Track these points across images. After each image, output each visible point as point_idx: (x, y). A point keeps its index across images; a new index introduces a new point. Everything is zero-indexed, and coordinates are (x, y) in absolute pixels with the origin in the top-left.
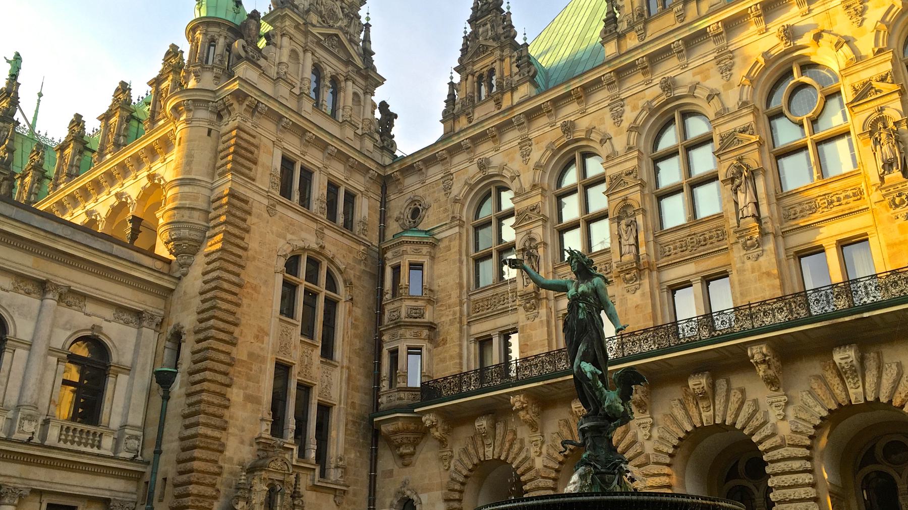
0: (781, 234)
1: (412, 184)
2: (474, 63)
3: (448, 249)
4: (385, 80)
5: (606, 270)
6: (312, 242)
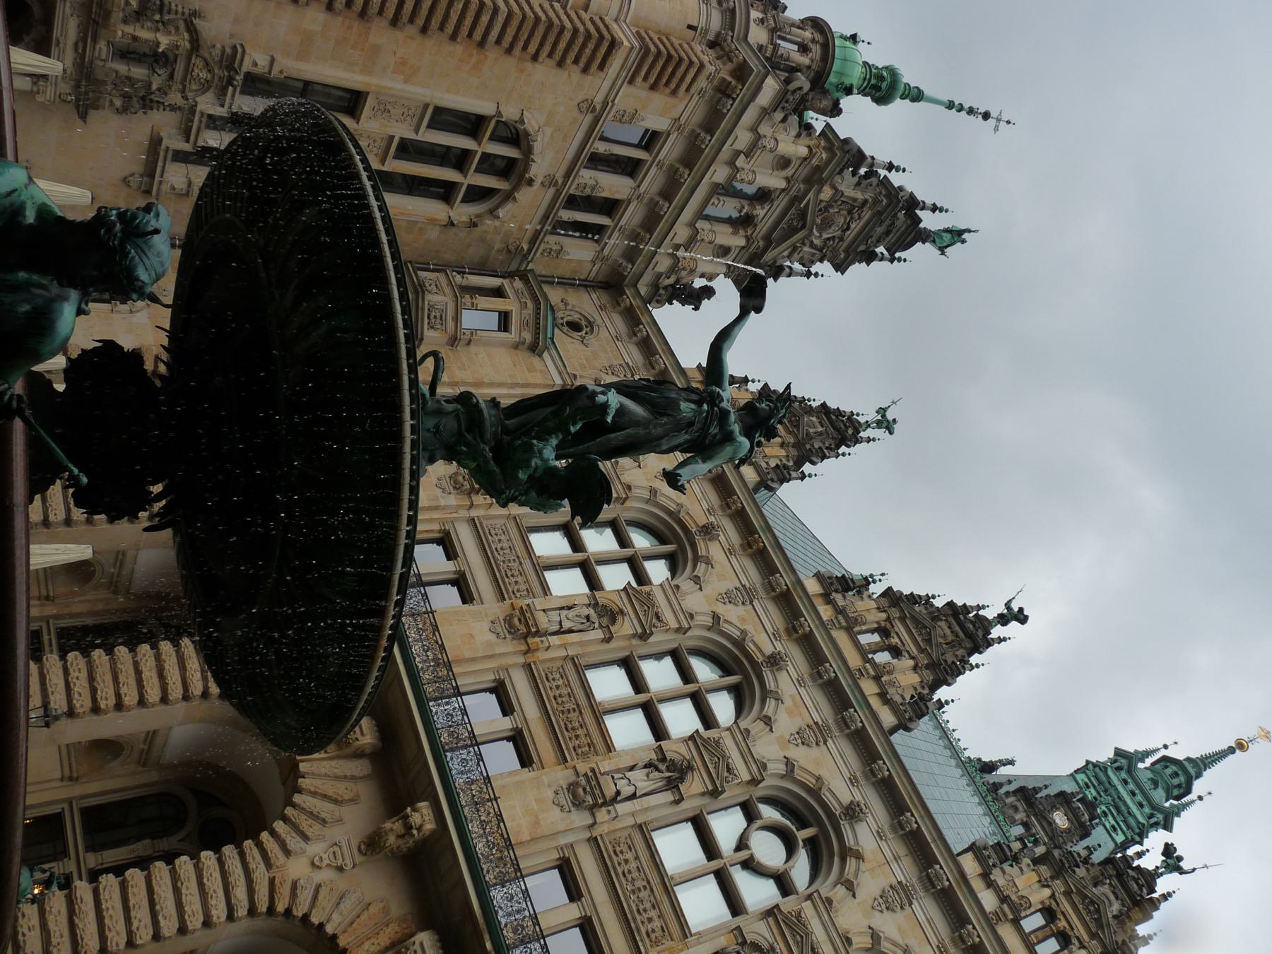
0: (594, 835)
1: (616, 323)
3: (531, 369)
5: (518, 591)
6: (538, 169)
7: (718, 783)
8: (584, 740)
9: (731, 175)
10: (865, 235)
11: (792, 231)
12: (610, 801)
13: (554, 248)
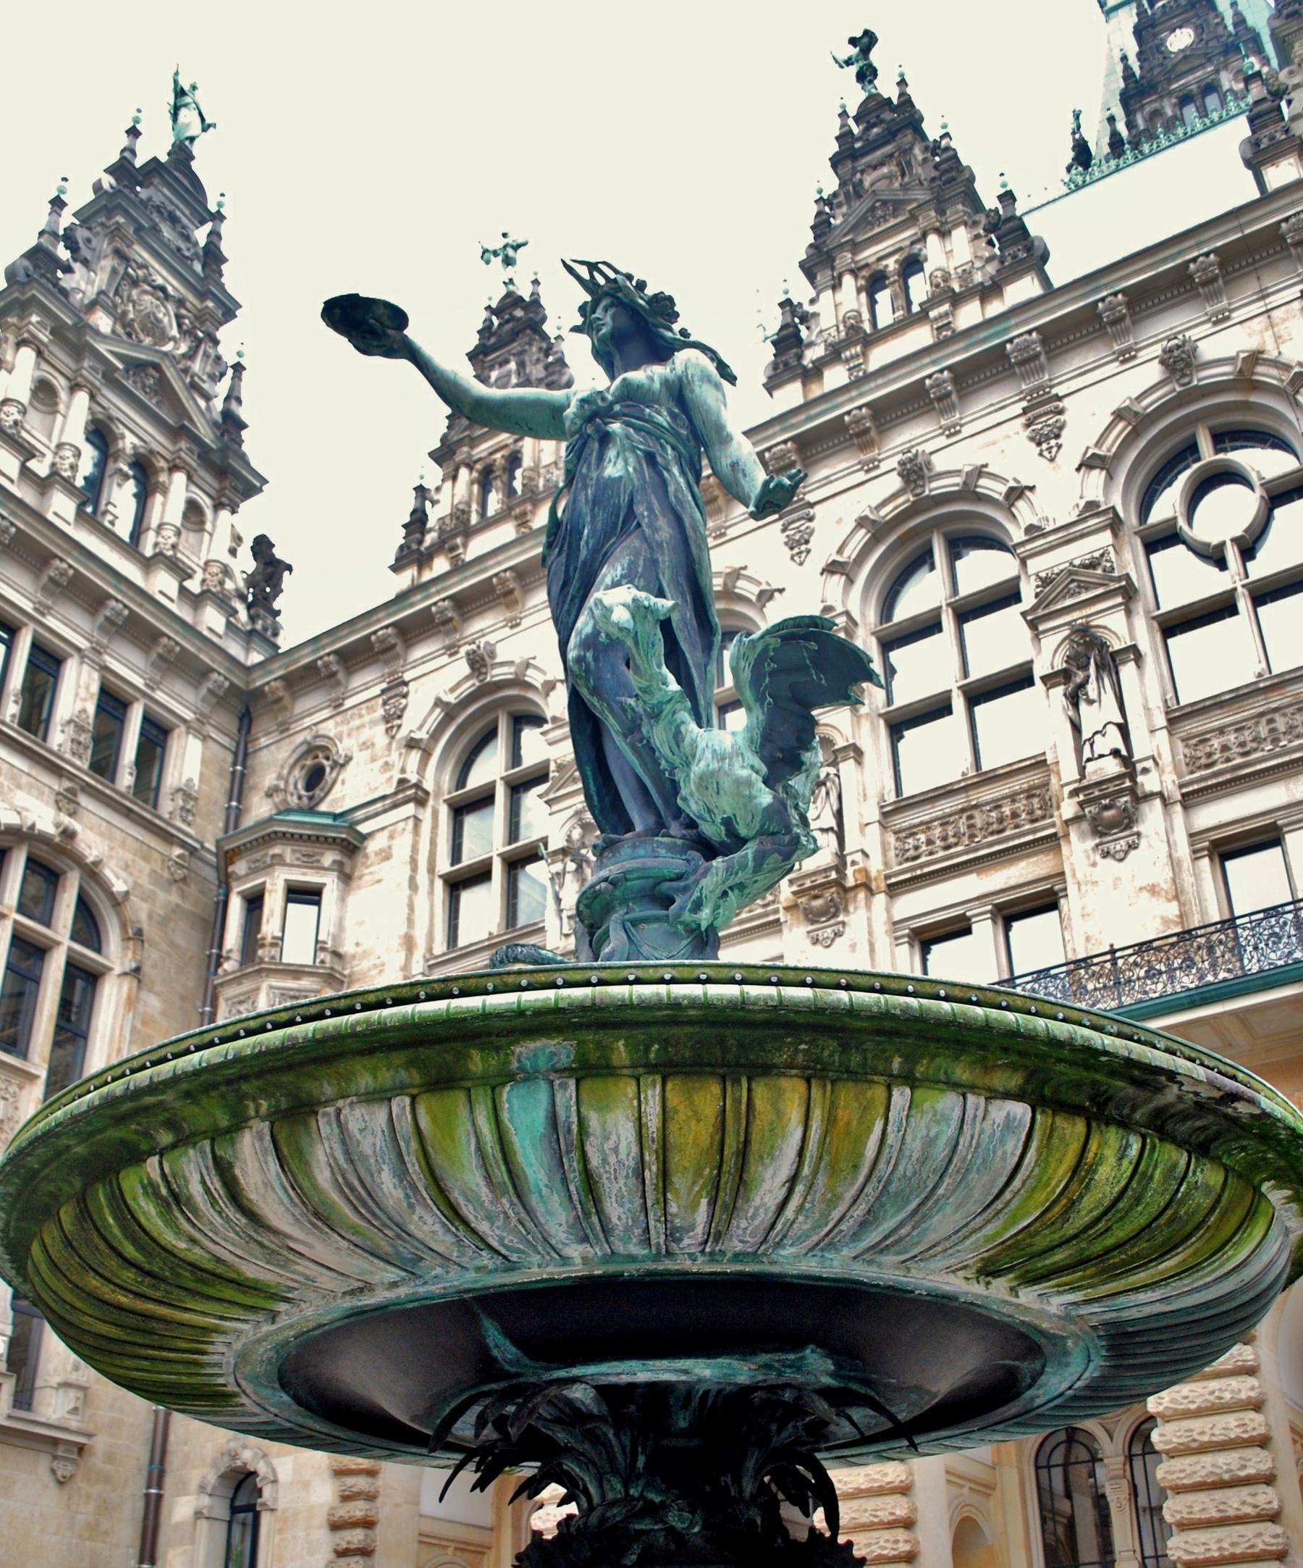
2: (473, 442)
3: (386, 855)
4: (266, 482)
7: (1113, 586)
8: (1021, 805)
9: (64, 487)
10: (176, 260)
11: (164, 387)
12: (1126, 767)
13: (181, 803)
